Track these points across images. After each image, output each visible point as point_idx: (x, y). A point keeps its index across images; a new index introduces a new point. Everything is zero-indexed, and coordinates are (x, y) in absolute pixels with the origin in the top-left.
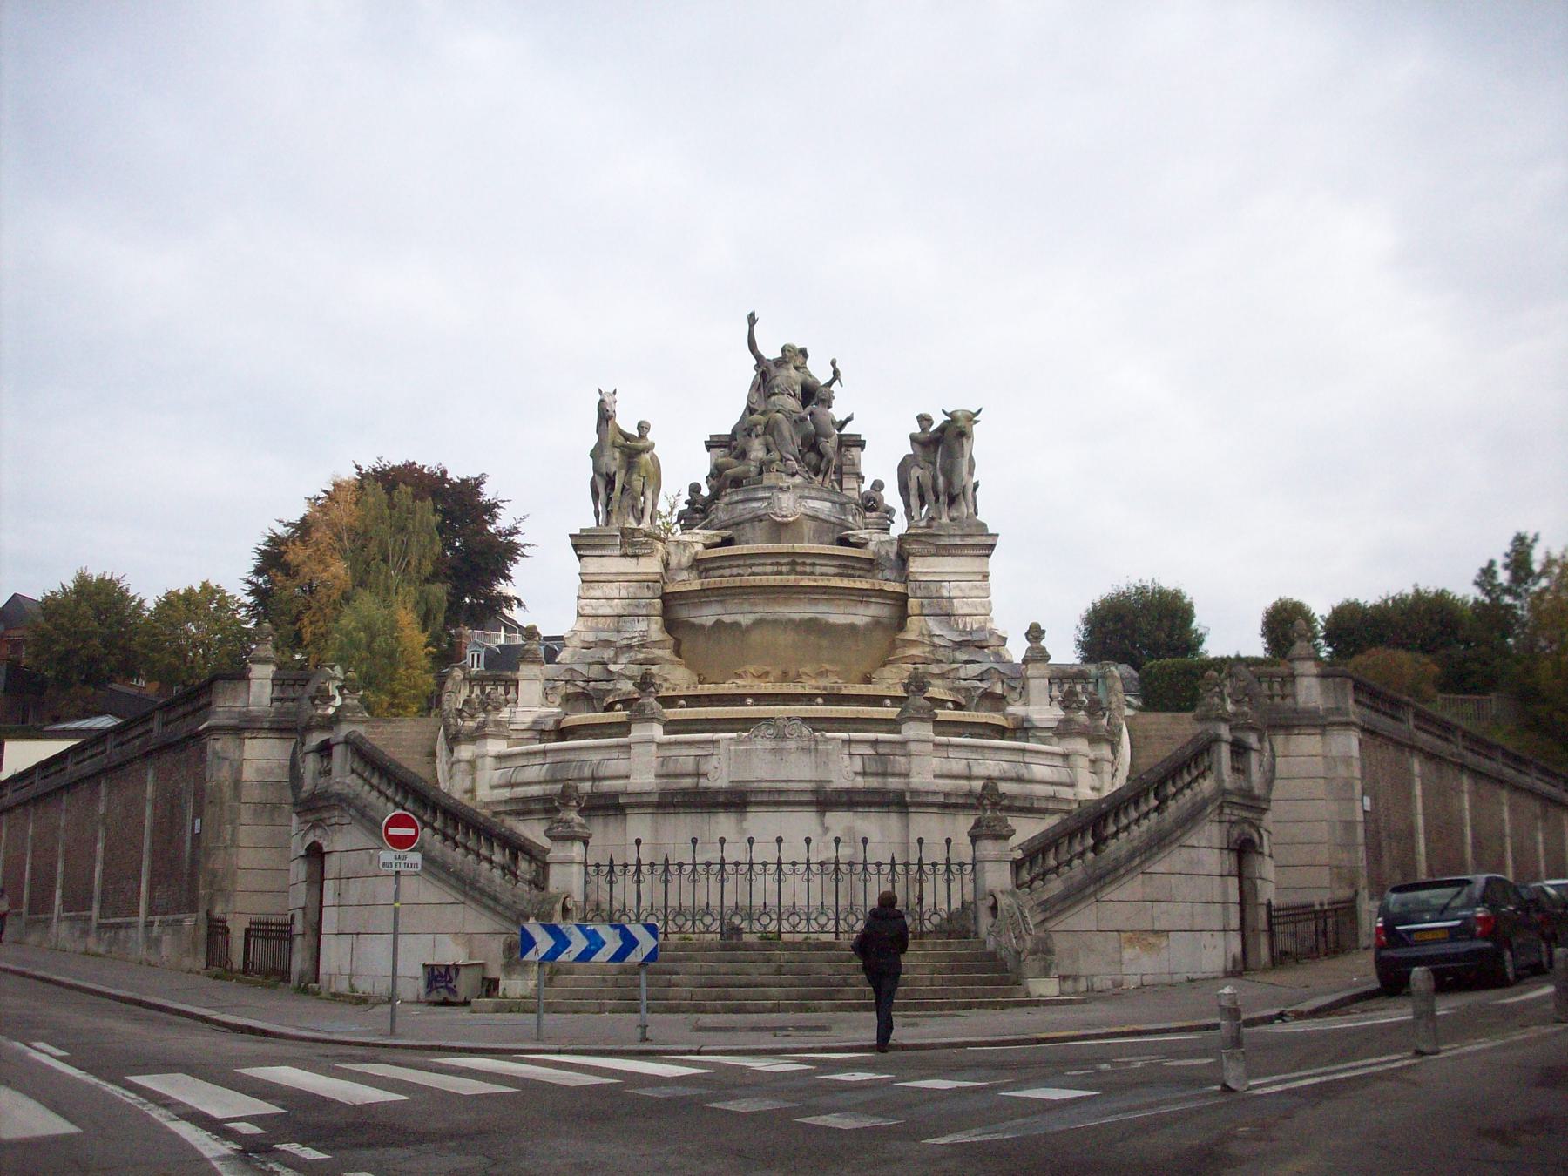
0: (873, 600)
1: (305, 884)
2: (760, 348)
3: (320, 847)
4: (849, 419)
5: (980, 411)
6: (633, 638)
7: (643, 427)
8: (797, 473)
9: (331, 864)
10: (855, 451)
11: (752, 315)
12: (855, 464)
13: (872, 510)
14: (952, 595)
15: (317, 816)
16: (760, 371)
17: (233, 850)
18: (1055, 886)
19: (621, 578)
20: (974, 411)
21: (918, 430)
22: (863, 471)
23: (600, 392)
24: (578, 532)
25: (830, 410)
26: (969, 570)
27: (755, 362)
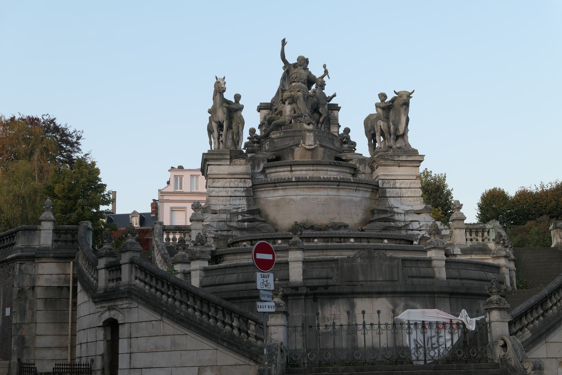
0: (362, 189)
1: (103, 342)
2: (286, 58)
3: (116, 321)
4: (334, 96)
5: (414, 91)
6: (239, 208)
7: (238, 97)
9: (123, 331)
10: (335, 112)
11: (284, 40)
12: (337, 119)
13: (345, 143)
14: (401, 186)
15: (111, 304)
16: (286, 69)
17: (33, 325)
18: (527, 334)
19: (230, 176)
20: (410, 92)
21: (379, 101)
22: (340, 122)
23: (216, 78)
24: (206, 152)
25: (323, 91)
26: (410, 173)
27: (283, 65)
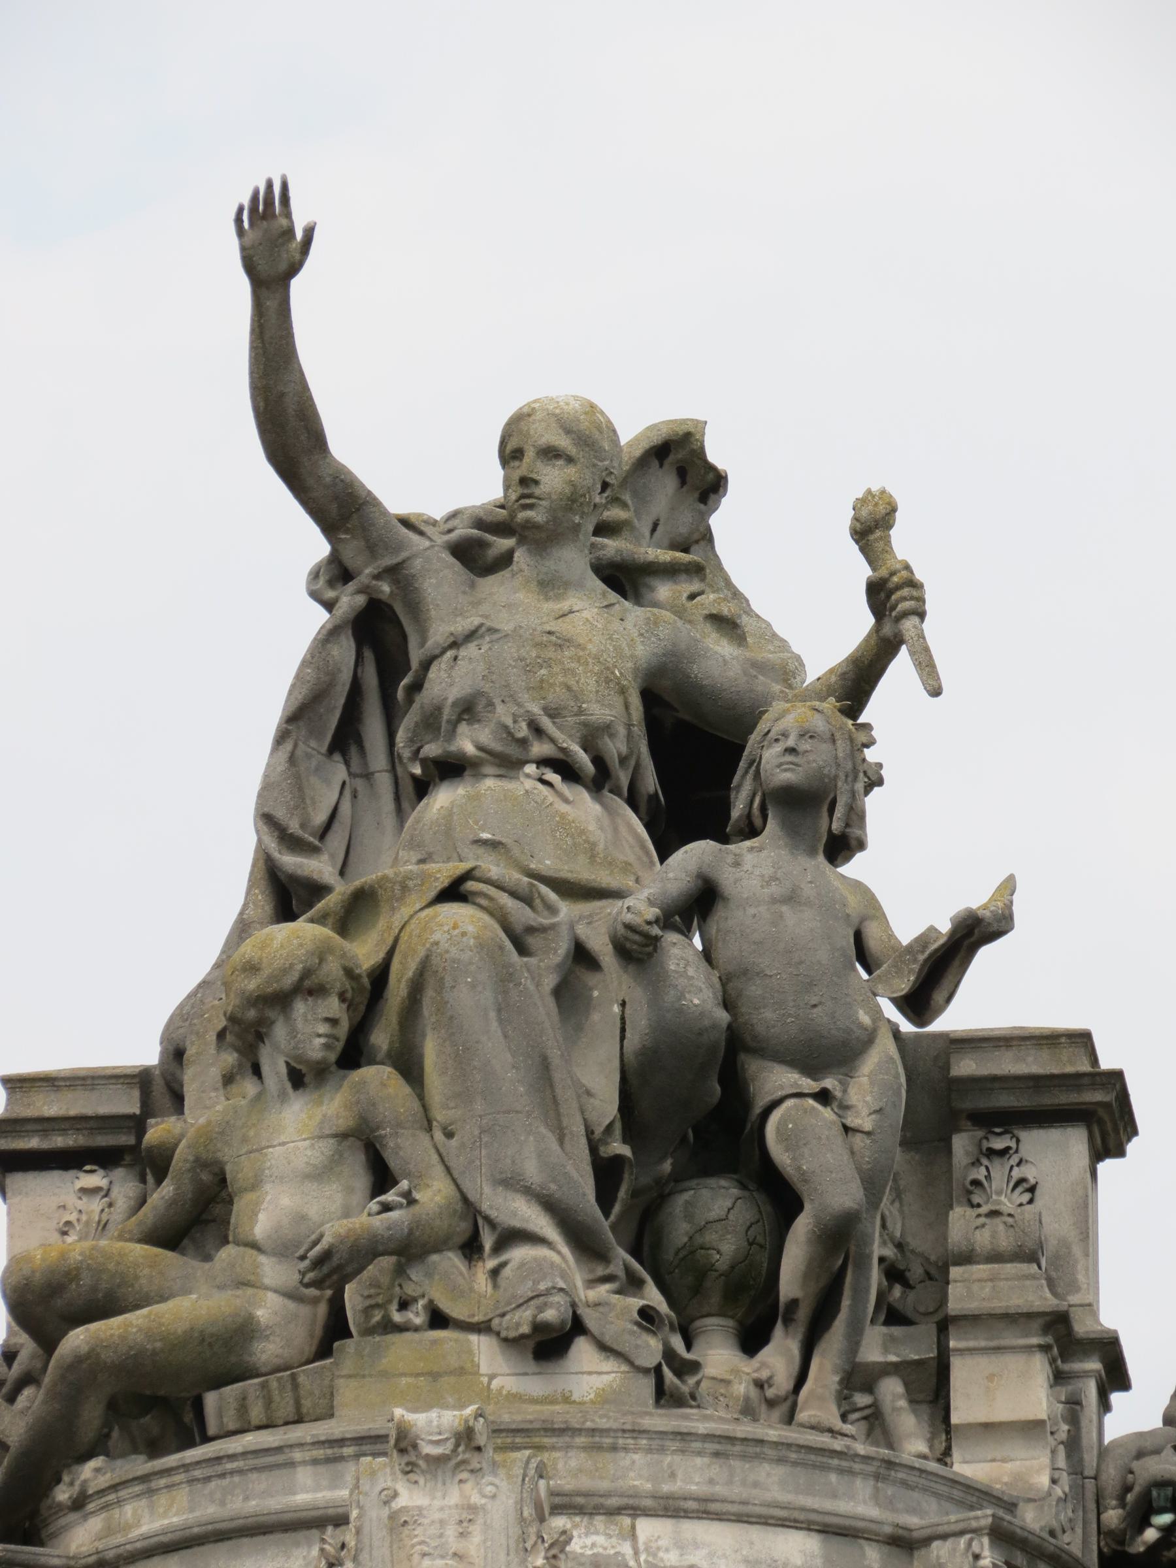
8: (577, 1327)
16: (350, 600)
25: (855, 868)
27: (318, 547)
